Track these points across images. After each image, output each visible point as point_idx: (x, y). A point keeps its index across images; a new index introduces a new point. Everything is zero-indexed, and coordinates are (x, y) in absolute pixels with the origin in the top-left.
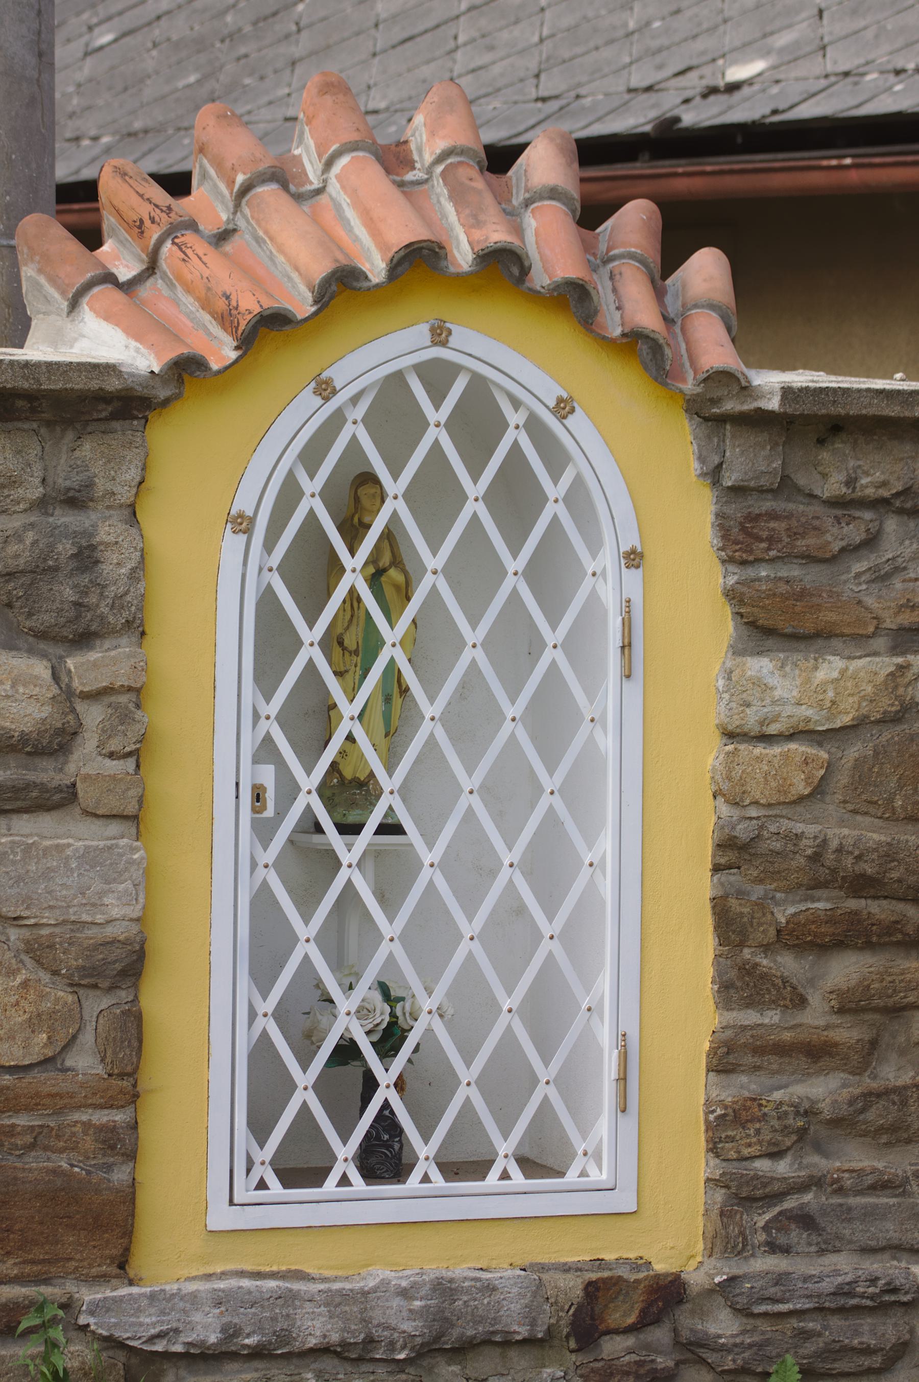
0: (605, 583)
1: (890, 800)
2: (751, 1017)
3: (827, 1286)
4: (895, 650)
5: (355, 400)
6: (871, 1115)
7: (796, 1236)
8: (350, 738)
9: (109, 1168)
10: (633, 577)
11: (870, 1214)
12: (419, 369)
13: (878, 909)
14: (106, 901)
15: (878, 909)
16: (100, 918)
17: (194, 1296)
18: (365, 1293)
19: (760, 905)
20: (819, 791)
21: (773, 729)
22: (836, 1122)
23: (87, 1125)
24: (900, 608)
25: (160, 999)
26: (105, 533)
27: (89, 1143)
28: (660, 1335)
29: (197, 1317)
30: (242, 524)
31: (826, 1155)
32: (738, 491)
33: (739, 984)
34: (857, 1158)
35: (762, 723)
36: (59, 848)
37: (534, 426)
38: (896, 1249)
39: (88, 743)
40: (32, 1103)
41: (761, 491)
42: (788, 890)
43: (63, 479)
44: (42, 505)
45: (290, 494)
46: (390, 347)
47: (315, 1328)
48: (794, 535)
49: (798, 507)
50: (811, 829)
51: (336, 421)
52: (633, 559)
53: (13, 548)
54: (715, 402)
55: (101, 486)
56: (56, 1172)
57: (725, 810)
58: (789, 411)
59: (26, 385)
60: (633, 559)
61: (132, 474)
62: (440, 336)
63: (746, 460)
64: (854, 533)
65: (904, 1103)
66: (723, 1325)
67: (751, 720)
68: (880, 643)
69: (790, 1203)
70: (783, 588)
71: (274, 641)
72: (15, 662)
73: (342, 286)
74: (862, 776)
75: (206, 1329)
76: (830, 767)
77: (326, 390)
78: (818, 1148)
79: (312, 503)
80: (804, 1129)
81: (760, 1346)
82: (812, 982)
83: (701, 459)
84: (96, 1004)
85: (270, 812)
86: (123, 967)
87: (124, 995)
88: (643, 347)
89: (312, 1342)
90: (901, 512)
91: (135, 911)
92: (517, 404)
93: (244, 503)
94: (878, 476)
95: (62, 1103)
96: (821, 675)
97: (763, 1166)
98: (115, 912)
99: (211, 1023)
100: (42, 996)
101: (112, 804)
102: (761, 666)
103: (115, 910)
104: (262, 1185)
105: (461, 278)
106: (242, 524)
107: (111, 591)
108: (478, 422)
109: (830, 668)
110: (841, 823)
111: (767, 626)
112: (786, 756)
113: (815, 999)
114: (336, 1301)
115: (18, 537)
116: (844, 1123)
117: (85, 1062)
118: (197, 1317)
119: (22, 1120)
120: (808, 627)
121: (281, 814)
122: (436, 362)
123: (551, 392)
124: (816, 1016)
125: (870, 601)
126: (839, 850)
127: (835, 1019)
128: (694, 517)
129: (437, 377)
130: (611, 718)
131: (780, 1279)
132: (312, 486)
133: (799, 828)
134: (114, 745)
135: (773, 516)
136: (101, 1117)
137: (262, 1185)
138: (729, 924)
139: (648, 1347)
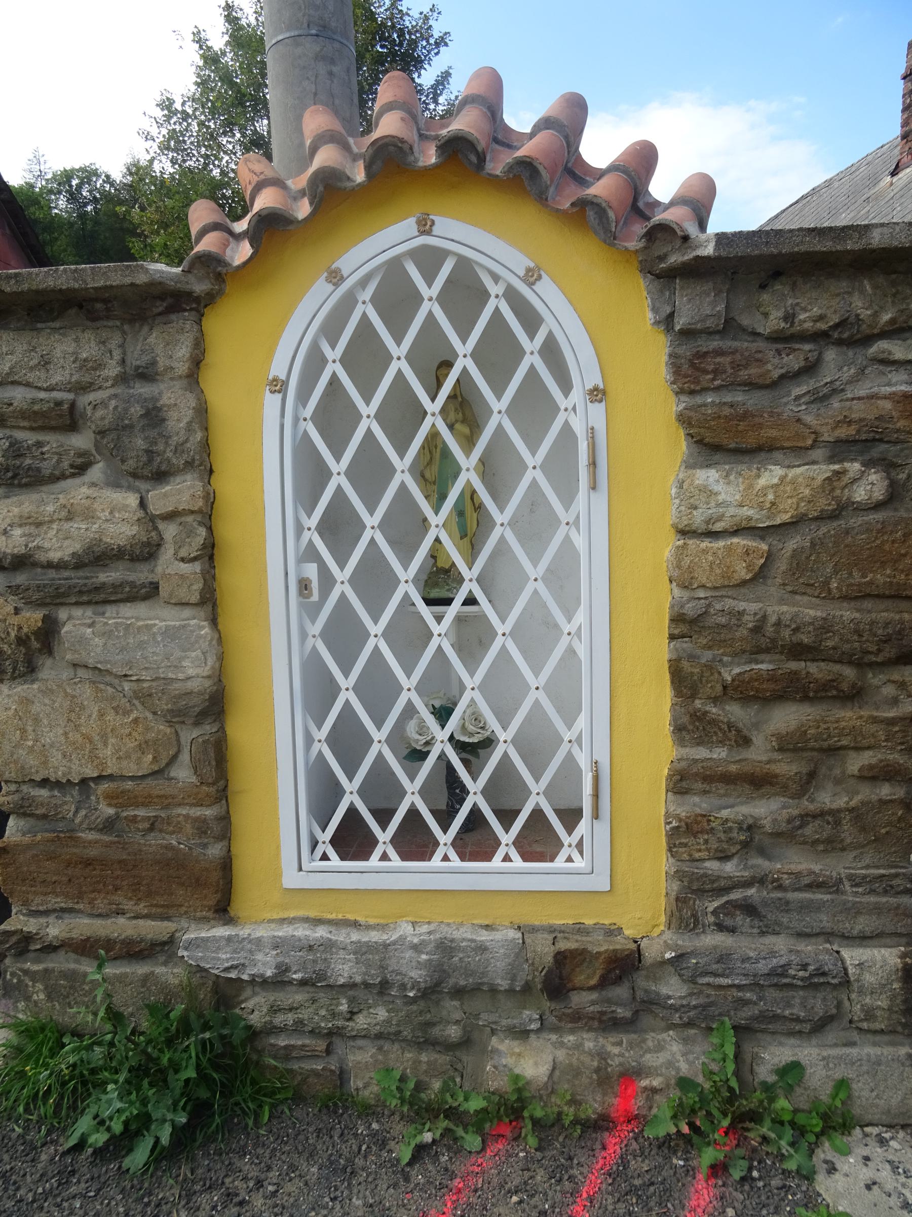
0: (577, 414)
1: (827, 583)
2: (701, 753)
3: (763, 967)
4: (831, 459)
5: (363, 283)
6: (808, 831)
7: (740, 919)
8: (437, 540)
9: (205, 846)
10: (597, 411)
11: (806, 907)
13: (816, 670)
14: (184, 664)
15: (816, 670)
16: (181, 676)
17: (259, 940)
18: (386, 946)
19: (709, 667)
20: (761, 575)
21: (718, 527)
22: (777, 835)
23: (187, 817)
24: (838, 424)
25: (241, 731)
26: (167, 399)
27: (188, 828)
28: (621, 992)
29: (259, 956)
30: (279, 386)
31: (769, 858)
32: (687, 334)
33: (691, 726)
34: (797, 862)
35: (707, 522)
36: (149, 627)
37: (511, 295)
38: (828, 935)
39: (167, 554)
40: (147, 801)
41: (710, 333)
42: (735, 655)
43: (136, 359)
44: (123, 379)
45: (315, 361)
46: (389, 238)
47: (344, 969)
48: (736, 366)
49: (744, 344)
50: (753, 607)
52: (597, 394)
53: (100, 413)
54: (662, 258)
55: (162, 363)
56: (169, 847)
57: (677, 592)
58: (723, 254)
59: (77, 286)
60: (597, 394)
61: (183, 351)
62: (425, 227)
63: (696, 305)
64: (794, 362)
65: (838, 823)
66: (672, 989)
67: (698, 519)
68: (818, 454)
69: (736, 895)
70: (727, 411)
72: (115, 496)
73: (329, 190)
74: (799, 564)
75: (265, 965)
76: (770, 557)
77: (336, 277)
78: (762, 852)
80: (750, 839)
81: (705, 1007)
82: (756, 726)
83: (655, 310)
84: (188, 735)
85: (315, 597)
86: (215, 706)
87: (208, 728)
88: (591, 214)
89: (341, 981)
90: (840, 343)
91: (206, 671)
92: (496, 278)
93: (278, 369)
94: (816, 311)
95: (167, 802)
96: (762, 482)
97: (713, 866)
98: (191, 672)
99: (279, 747)
100: (147, 729)
101: (183, 594)
102: (709, 477)
104: (325, 857)
105: (428, 171)
106: (279, 386)
107: (174, 440)
108: (465, 292)
109: (771, 475)
110: (782, 601)
111: (716, 442)
112: (729, 549)
113: (758, 740)
114: (361, 951)
115: (104, 404)
116: (788, 835)
117: (183, 773)
118: (259, 956)
119: (141, 812)
120: (751, 441)
122: (425, 248)
123: (519, 262)
124: (759, 753)
125: (809, 419)
126: (778, 624)
127: (777, 756)
128: (649, 357)
129: (429, 260)
130: (587, 525)
131: (723, 958)
132: (334, 354)
133: (742, 606)
134: (183, 553)
135: (719, 353)
136: (196, 812)
137: (325, 857)
138: (683, 681)
139: (609, 1001)
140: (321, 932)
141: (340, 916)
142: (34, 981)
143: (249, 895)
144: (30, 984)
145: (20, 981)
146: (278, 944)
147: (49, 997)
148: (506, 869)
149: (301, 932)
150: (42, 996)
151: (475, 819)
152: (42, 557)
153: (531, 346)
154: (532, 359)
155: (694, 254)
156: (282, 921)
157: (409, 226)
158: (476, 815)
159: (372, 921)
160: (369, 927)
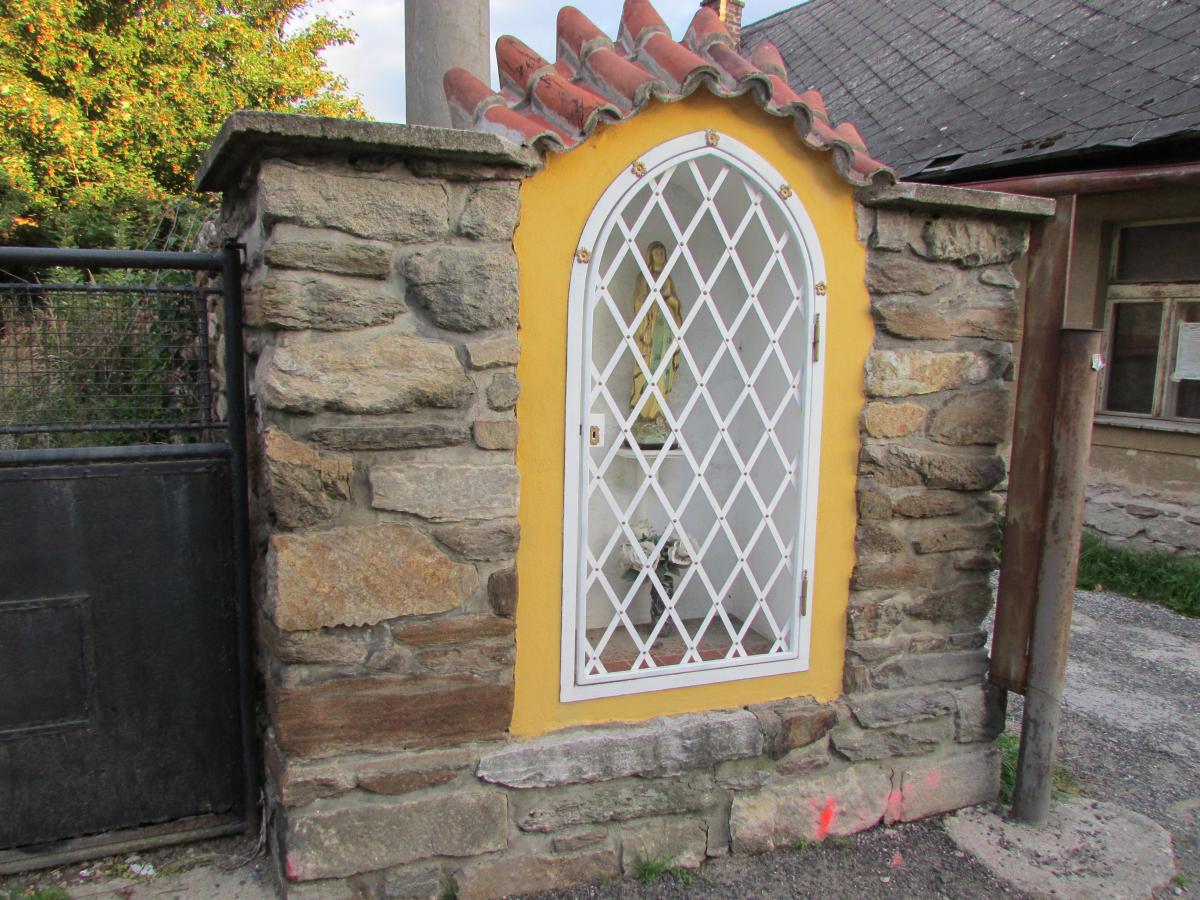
5: (658, 179)
7: (891, 679)
12: (698, 161)
14: (494, 505)
16: (488, 517)
33: (868, 539)
37: (768, 205)
45: (616, 239)
51: (646, 192)
58: (920, 199)
59: (429, 145)
70: (904, 310)
71: (608, 335)
72: (429, 345)
77: (640, 171)
79: (630, 246)
98: (500, 512)
103: (498, 514)
104: (594, 671)
112: (904, 409)
118: (552, 765)
121: (609, 445)
122: (710, 156)
132: (630, 234)
140: (600, 736)
141: (608, 720)
142: (326, 827)
143: (526, 714)
144: (322, 831)
145: (311, 830)
146: (568, 753)
147: (343, 841)
148: (738, 665)
149: (586, 737)
150: (335, 841)
151: (670, 629)
152: (351, 403)
153: (777, 246)
154: (778, 257)
155: (900, 195)
156: (561, 732)
157: (697, 139)
158: (670, 625)
159: (634, 721)
160: (633, 726)
